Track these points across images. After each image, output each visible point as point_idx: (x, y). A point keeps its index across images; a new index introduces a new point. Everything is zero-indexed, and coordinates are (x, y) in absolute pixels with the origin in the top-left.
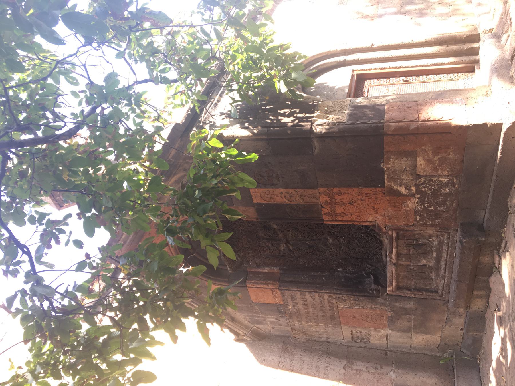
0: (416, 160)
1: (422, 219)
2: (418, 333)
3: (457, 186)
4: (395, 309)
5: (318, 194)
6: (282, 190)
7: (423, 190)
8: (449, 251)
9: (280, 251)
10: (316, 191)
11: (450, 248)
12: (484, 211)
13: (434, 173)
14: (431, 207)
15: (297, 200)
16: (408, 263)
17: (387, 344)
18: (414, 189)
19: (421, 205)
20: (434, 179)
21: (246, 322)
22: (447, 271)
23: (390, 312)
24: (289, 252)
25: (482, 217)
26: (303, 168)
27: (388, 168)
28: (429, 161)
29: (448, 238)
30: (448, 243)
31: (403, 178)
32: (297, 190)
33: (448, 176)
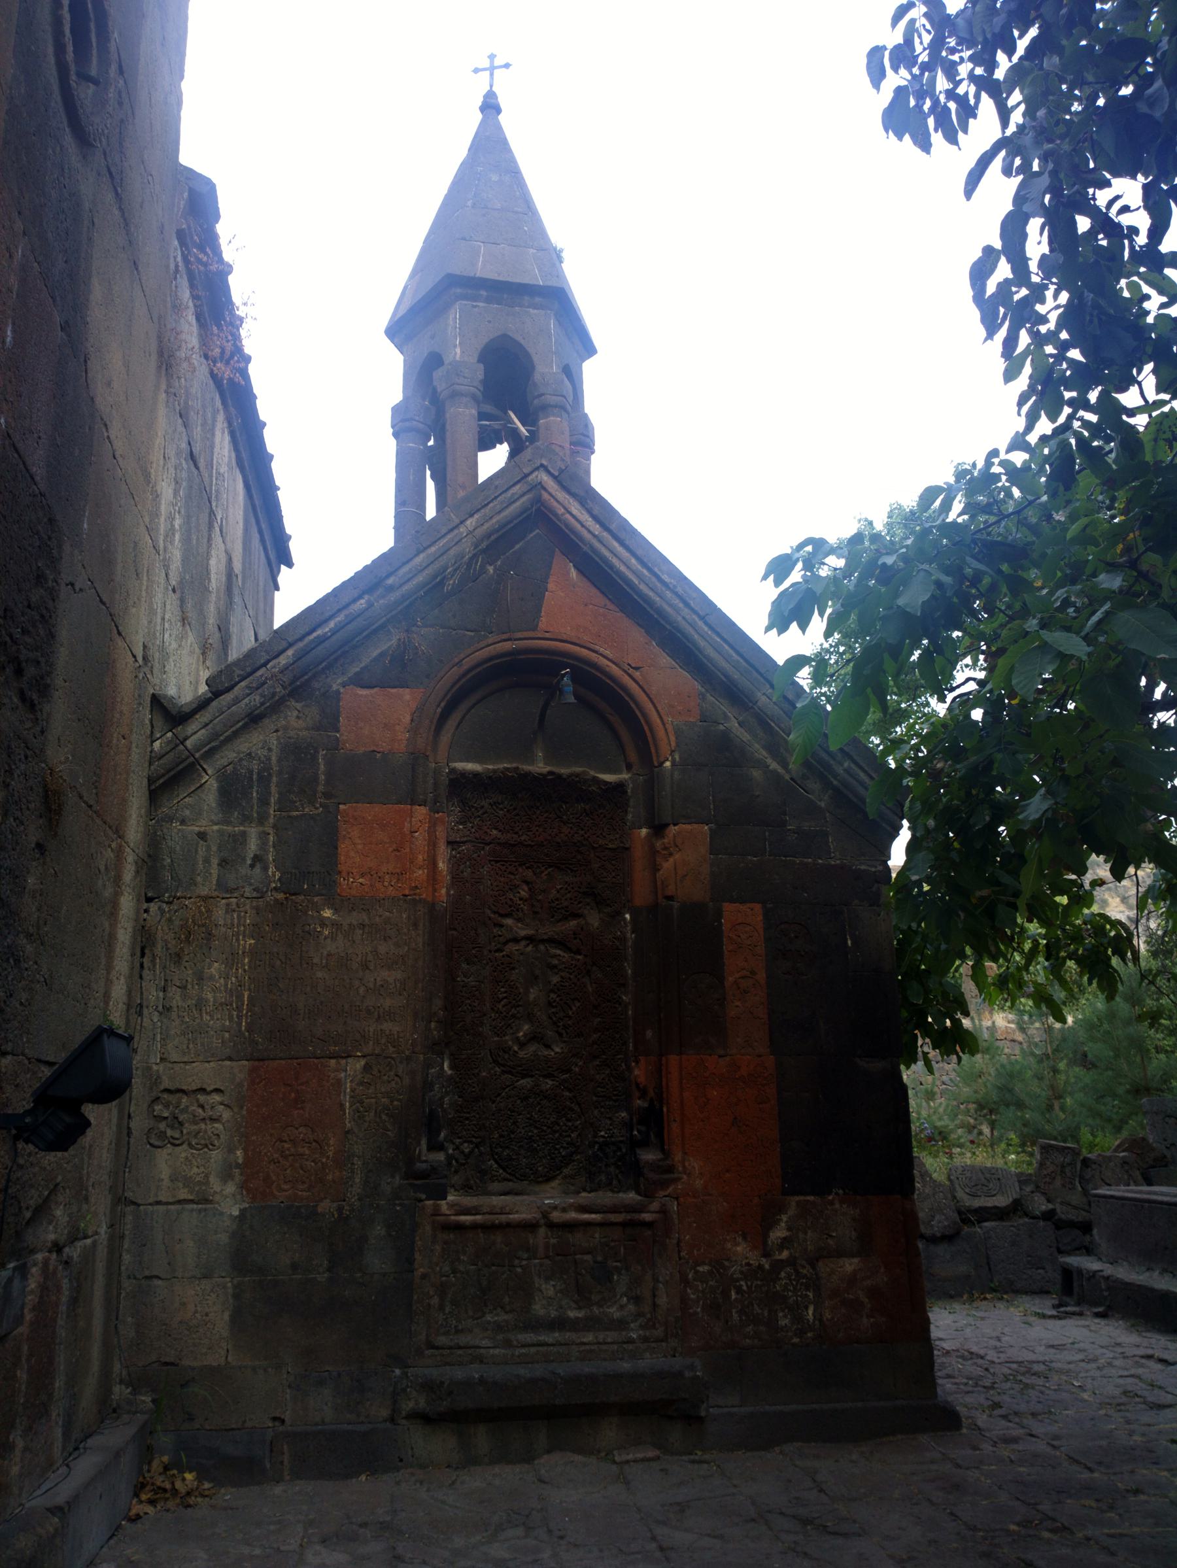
0: (853, 1256)
2: (236, 1296)
3: (796, 1340)
7: (783, 1274)
8: (604, 1347)
11: (616, 1347)
14: (737, 1293)
17: (158, 1203)
18: (785, 1254)
19: (741, 1272)
20: (811, 1295)
22: (533, 1350)
23: (340, 1209)
27: (832, 1203)
29: (645, 1340)
30: (630, 1341)
31: (809, 1233)
33: (821, 1321)
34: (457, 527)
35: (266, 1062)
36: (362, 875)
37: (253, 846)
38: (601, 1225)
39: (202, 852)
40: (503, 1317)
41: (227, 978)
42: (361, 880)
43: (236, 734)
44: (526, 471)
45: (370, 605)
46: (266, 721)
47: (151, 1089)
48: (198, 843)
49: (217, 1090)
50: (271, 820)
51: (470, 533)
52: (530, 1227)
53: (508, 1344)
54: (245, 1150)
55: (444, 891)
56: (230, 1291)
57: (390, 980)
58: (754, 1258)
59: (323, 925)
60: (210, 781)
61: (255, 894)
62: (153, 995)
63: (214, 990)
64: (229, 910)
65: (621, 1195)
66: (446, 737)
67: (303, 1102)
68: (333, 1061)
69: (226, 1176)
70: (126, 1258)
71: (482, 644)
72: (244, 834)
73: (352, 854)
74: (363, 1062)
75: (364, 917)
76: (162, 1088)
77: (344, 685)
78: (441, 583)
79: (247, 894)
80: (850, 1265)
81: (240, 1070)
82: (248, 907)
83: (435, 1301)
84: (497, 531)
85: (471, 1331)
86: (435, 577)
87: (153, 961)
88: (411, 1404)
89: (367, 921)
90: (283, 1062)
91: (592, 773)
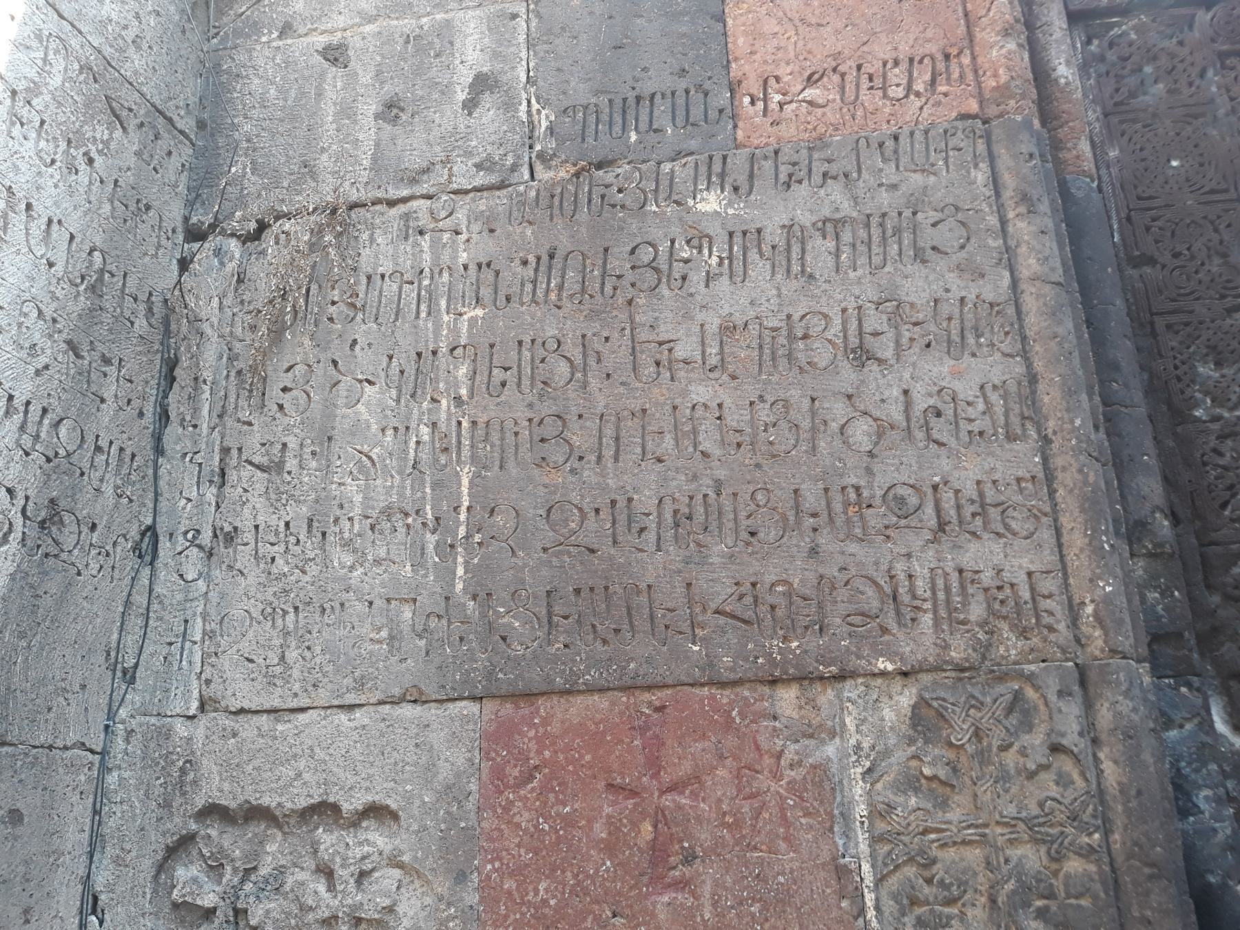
35: (543, 705)
36: (810, 81)
42: (810, 93)
47: (167, 805)
48: (322, 76)
49: (375, 811)
57: (966, 389)
61: (481, 179)
62: (187, 501)
63: (367, 466)
67: (689, 858)
68: (787, 698)
72: (446, 31)
73: (770, 26)
74: (906, 698)
75: (836, 198)
76: (200, 802)
79: (461, 182)
82: (461, 215)
87: (193, 398)
89: (847, 208)
90: (600, 702)
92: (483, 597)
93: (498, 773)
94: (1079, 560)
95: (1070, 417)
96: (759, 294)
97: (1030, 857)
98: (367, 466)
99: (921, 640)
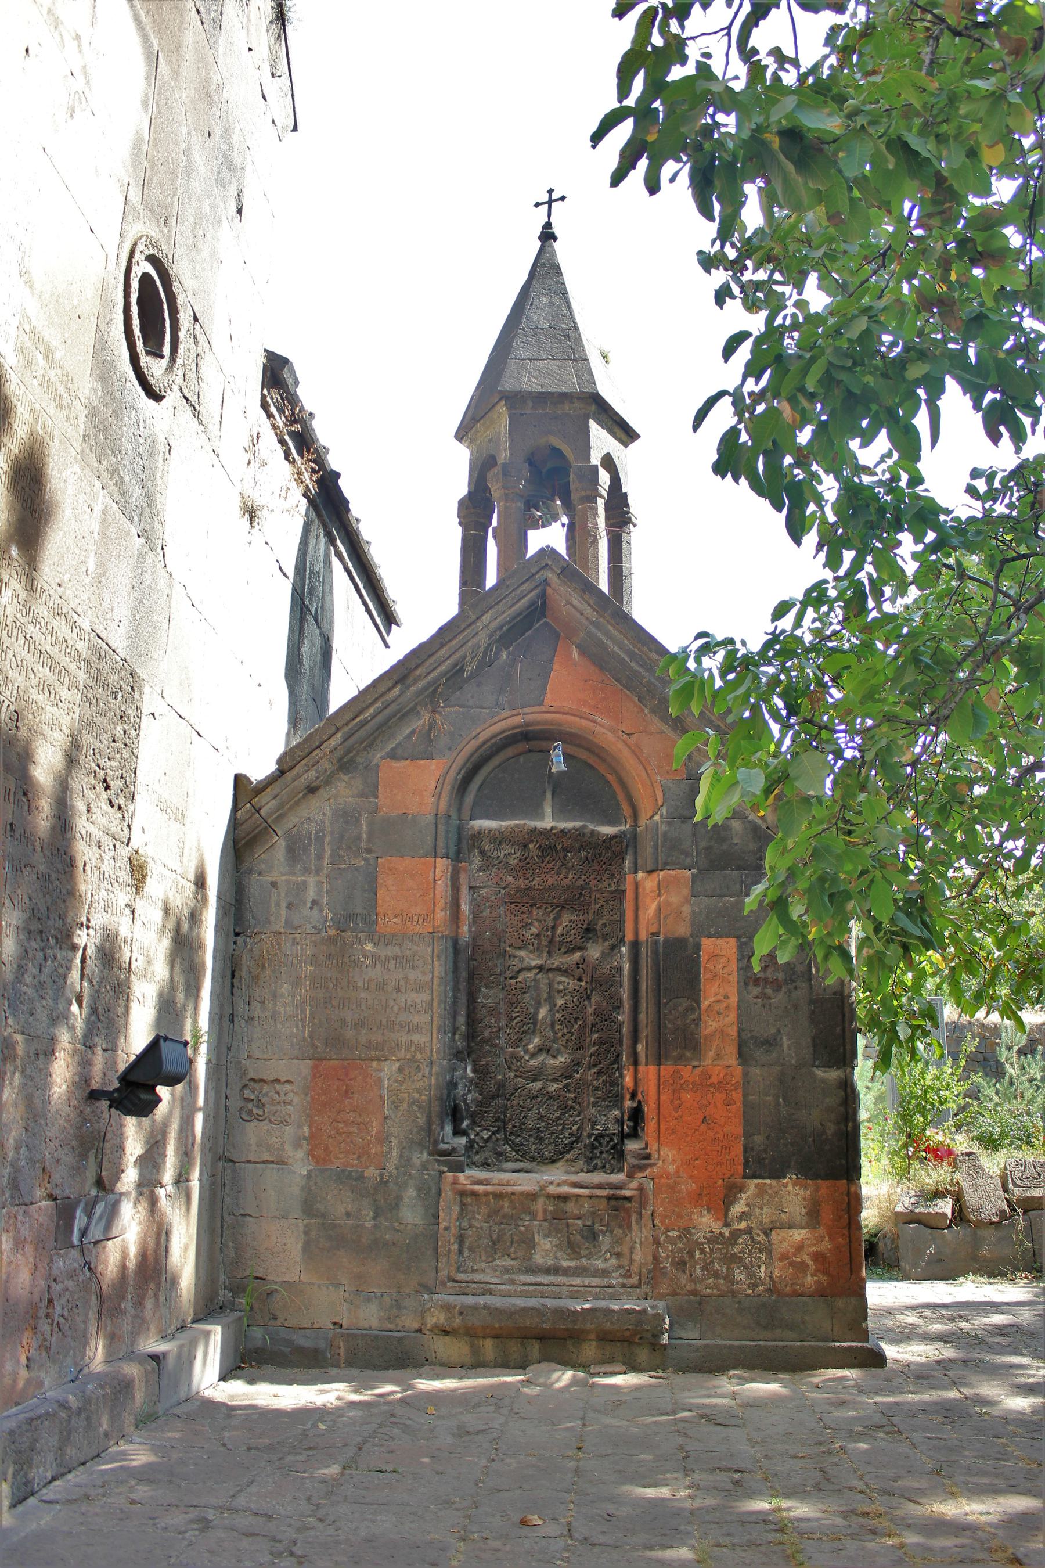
1: (671, 1241)
2: (306, 1233)
3: (749, 1292)
4: (391, 1185)
5: (726, 1063)
6: (734, 999)
7: (740, 1241)
9: (520, 948)
10: (733, 1061)
12: (697, 1336)
13: (776, 1255)
15: (710, 1025)
16: (540, 1216)
17: (249, 1162)
18: (743, 1225)
21: (295, 820)
22: (531, 1288)
23: (381, 1175)
24: (516, 969)
25: (683, 1335)
26: (785, 1046)
27: (785, 1186)
28: (800, 1248)
29: (624, 1286)
32: (735, 1028)
34: (474, 622)
36: (395, 916)
37: (311, 893)
38: (590, 1197)
39: (274, 897)
40: (508, 1262)
41: (294, 996)
43: (297, 803)
44: (533, 571)
45: (402, 693)
46: (321, 791)
49: (288, 1081)
50: (325, 872)
51: (487, 626)
52: (532, 1196)
53: (512, 1282)
54: (310, 1127)
55: (466, 928)
56: (301, 1229)
57: (418, 1001)
58: (717, 1227)
59: (365, 957)
60: (280, 844)
62: (241, 1008)
63: (285, 1005)
64: (295, 943)
65: (613, 1176)
66: (469, 799)
68: (375, 1064)
69: (297, 1145)
70: (228, 1200)
71: (496, 719)
74: (397, 1065)
75: (397, 949)
77: (382, 758)
78: (462, 670)
80: (798, 1235)
81: (305, 1067)
83: (455, 1247)
84: (509, 622)
85: (483, 1271)
86: (456, 665)
88: (434, 1320)
91: (592, 827)
92: (311, 1037)
93: (314, 1076)
94: (435, 1040)
95: (438, 1010)
96: (376, 973)
97: (416, 1095)
98: (285, 1005)
99: (402, 1054)
